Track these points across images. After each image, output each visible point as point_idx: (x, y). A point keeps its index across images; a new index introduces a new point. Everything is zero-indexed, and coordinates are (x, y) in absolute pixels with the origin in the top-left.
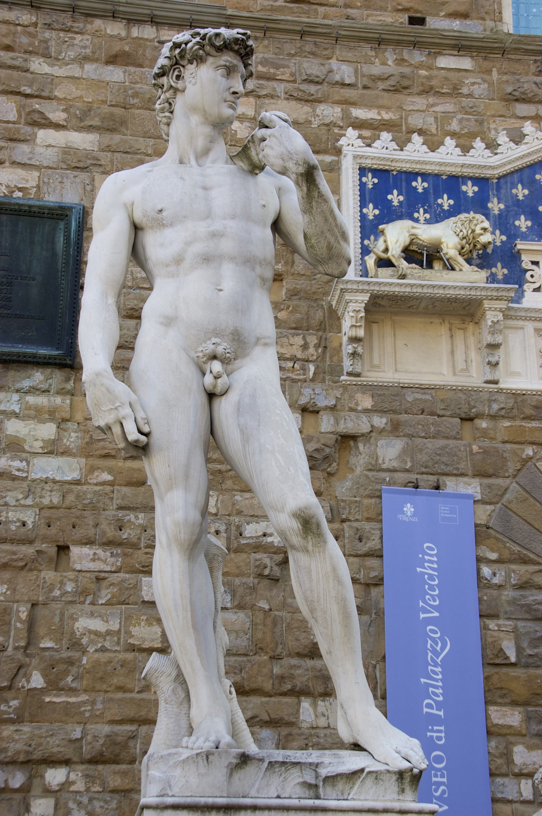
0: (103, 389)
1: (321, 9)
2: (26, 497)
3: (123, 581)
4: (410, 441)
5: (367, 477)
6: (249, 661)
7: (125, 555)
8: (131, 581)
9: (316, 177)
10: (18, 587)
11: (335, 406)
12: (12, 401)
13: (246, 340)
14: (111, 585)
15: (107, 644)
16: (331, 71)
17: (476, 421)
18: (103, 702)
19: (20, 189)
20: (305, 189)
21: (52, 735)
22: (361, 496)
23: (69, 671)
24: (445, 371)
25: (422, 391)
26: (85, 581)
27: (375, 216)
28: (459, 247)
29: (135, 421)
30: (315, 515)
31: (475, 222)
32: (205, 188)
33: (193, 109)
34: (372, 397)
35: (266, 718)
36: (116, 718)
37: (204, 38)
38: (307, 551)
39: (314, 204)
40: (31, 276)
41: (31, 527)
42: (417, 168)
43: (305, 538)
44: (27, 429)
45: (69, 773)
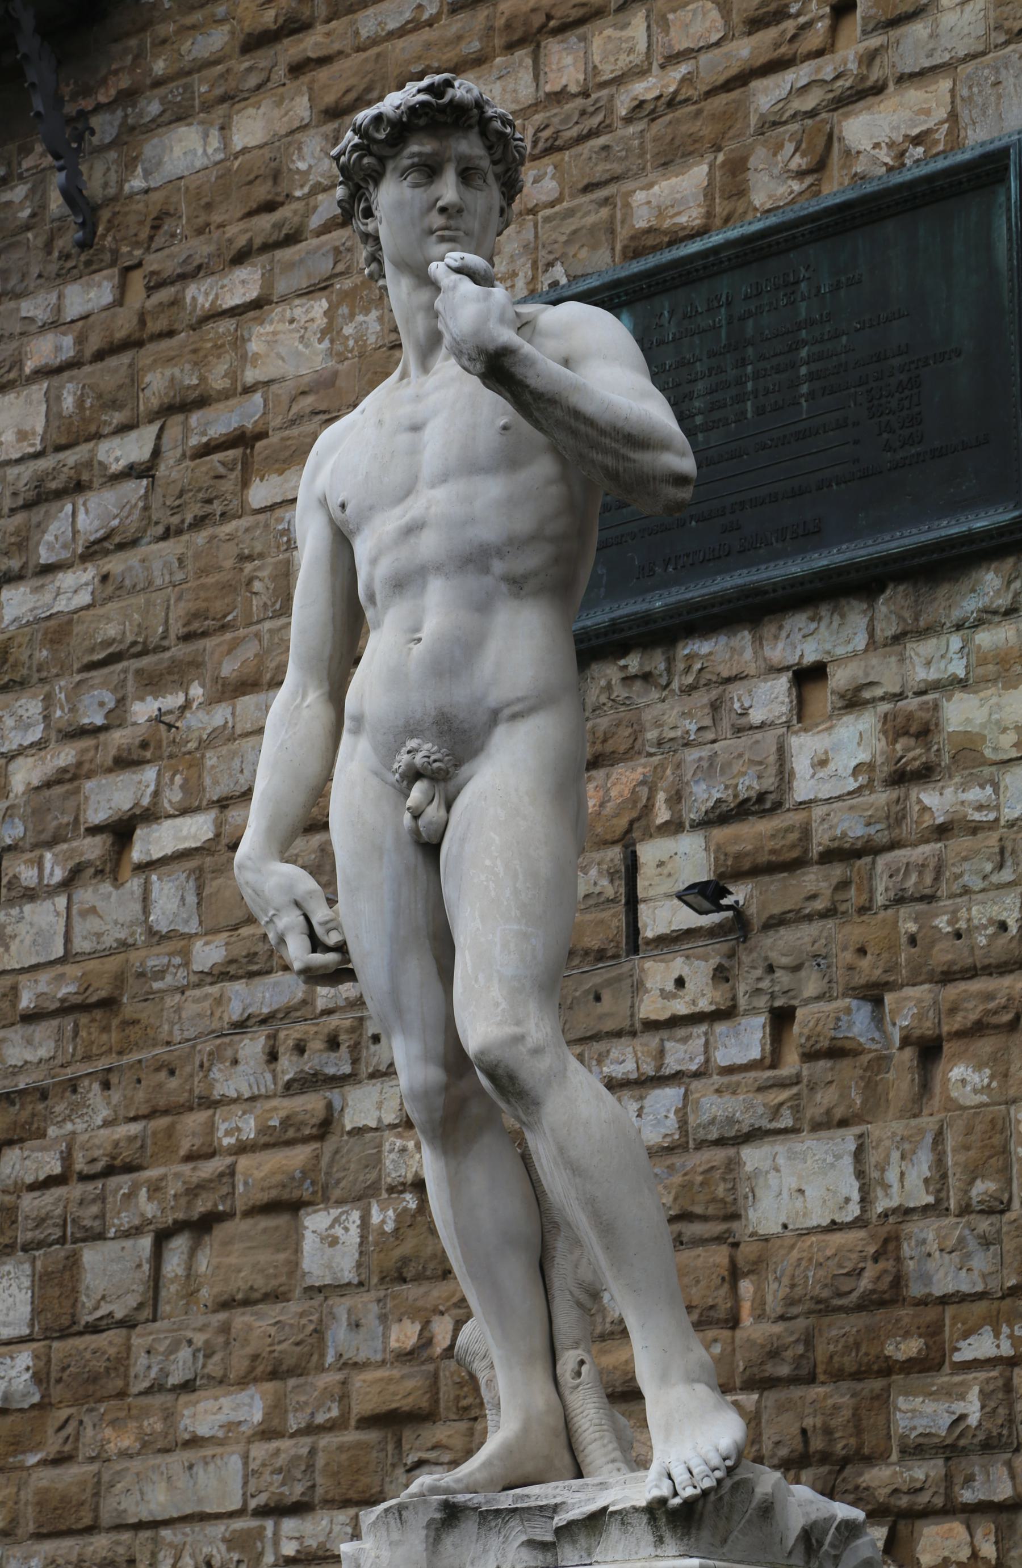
2: (1001, 866)
9: (513, 369)
10: (1012, 1069)
12: (950, 654)
13: (466, 726)
19: (917, 140)
30: (499, 1062)
39: (536, 414)
41: (1015, 931)
44: (985, 710)
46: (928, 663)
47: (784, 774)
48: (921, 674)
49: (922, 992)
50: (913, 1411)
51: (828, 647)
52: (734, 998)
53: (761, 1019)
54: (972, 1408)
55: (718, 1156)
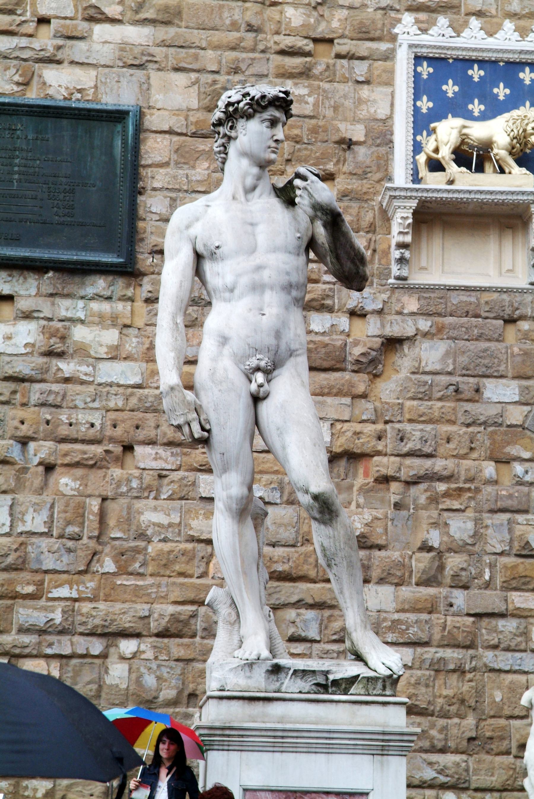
2: (94, 401)
3: (183, 479)
4: (453, 345)
5: (411, 379)
6: (297, 552)
7: (185, 454)
8: (190, 479)
10: (89, 484)
14: (172, 482)
15: (170, 536)
17: (518, 323)
18: (167, 586)
19: (80, 91)
21: (124, 613)
22: (404, 398)
23: (137, 559)
24: (491, 273)
25: (468, 293)
26: (148, 478)
27: (429, 109)
28: (510, 148)
31: (526, 122)
32: (252, 224)
33: (244, 154)
35: (311, 601)
36: (179, 600)
37: (252, 99)
40: (92, 182)
42: (474, 55)
45: (139, 644)
46: (67, 309)
48: (64, 313)
50: (27, 615)
51: (16, 289)
54: (58, 617)
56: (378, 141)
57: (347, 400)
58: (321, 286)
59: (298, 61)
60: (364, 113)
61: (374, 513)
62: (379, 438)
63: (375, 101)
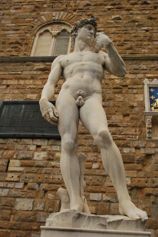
0: (44, 104)
1: (138, 55)
5: (155, 165)
8: (87, 194)
11: (145, 146)
16: (140, 67)
20: (109, 50)
27: (154, 98)
29: (53, 113)
32: (81, 55)
33: (81, 38)
34: (155, 144)
38: (105, 148)
43: (104, 143)
46: (55, 148)
47: (33, 156)
48: (54, 149)
49: (47, 184)
52: (20, 180)
53: (23, 183)
55: (13, 199)
56: (141, 106)
57: (136, 171)
58: (126, 141)
59: (118, 90)
60: (136, 100)
61: (146, 205)
62: (146, 182)
63: (139, 97)
